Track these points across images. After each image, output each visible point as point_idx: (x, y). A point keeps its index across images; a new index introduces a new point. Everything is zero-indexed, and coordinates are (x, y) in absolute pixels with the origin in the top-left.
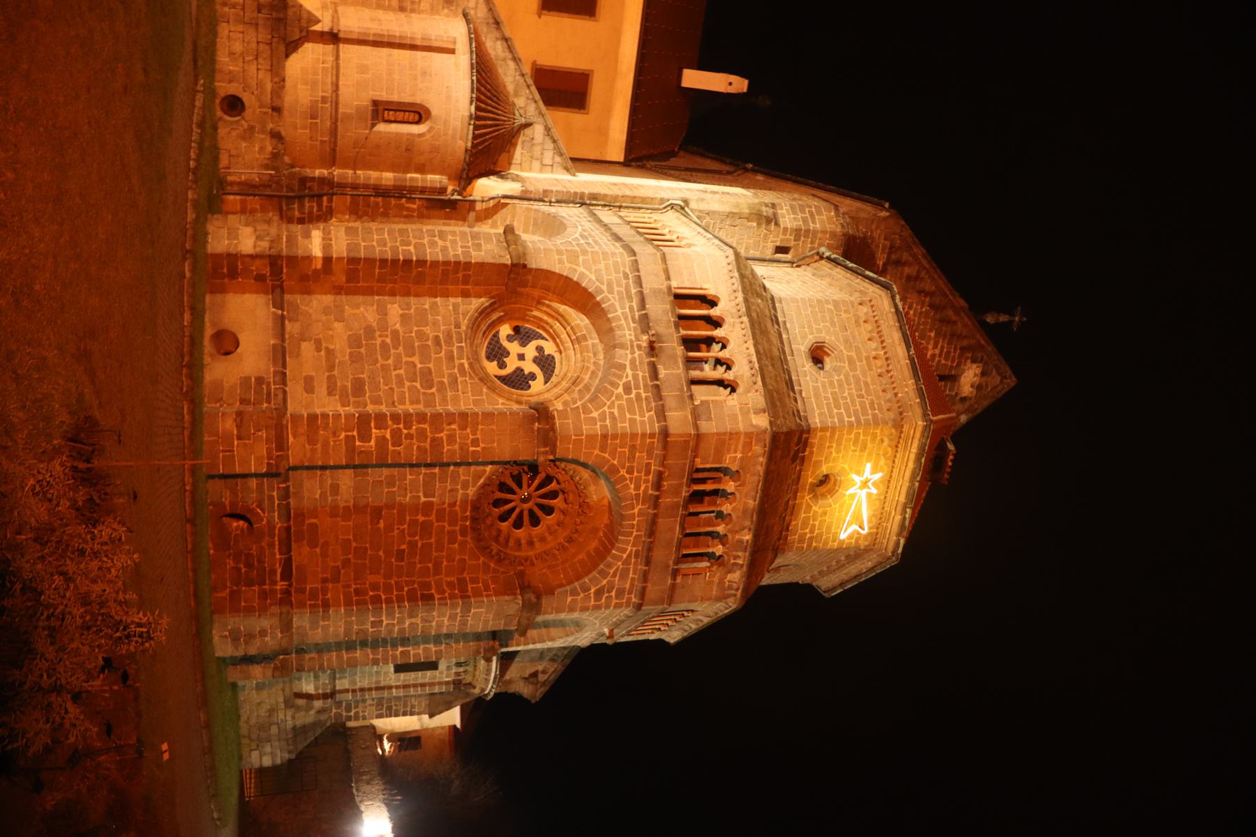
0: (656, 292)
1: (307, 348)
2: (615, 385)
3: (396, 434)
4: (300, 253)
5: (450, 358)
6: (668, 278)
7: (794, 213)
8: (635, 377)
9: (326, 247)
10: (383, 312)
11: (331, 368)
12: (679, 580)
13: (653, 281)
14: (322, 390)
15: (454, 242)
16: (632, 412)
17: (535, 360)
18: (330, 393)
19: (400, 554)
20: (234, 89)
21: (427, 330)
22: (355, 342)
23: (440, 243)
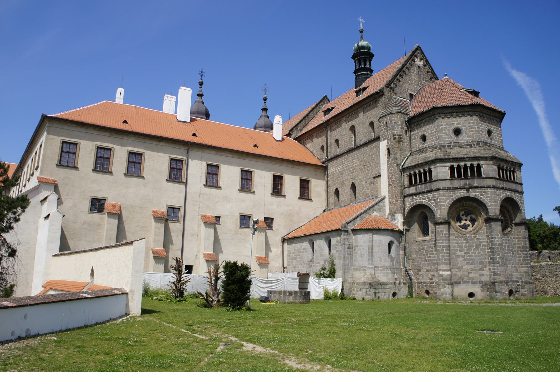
0: (451, 184)
1: (471, 275)
2: (481, 198)
3: (499, 255)
4: (448, 277)
5: (472, 239)
6: (447, 180)
7: (395, 128)
8: (478, 192)
9: (446, 270)
10: (459, 256)
11: (476, 270)
12: (518, 181)
13: (447, 184)
14: (483, 272)
15: (441, 237)
16: (488, 194)
17: (466, 216)
18: (484, 270)
19: (513, 253)
20: (391, 295)
21: (464, 245)
22: (468, 263)
23: (441, 241)
